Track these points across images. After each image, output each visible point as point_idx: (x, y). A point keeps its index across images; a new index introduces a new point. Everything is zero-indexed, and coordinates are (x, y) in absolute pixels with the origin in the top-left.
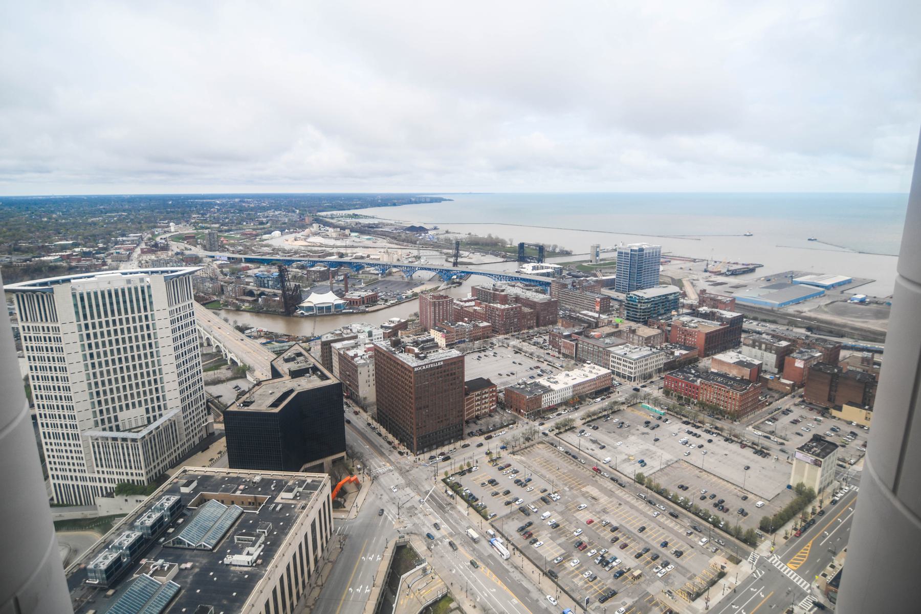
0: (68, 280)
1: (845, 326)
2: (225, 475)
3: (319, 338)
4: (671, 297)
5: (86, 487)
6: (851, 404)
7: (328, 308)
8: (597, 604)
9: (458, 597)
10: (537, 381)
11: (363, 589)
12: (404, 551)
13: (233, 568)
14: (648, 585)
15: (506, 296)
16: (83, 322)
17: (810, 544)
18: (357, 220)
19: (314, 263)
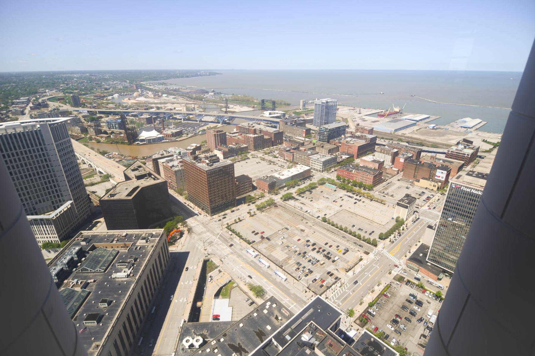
1: (425, 140)
2: (105, 233)
3: (150, 157)
4: (342, 128)
6: (424, 178)
8: (304, 278)
9: (237, 281)
10: (273, 175)
11: (189, 282)
12: (208, 263)
13: (117, 279)
14: (327, 267)
15: (255, 130)
17: (400, 243)
18: (166, 87)
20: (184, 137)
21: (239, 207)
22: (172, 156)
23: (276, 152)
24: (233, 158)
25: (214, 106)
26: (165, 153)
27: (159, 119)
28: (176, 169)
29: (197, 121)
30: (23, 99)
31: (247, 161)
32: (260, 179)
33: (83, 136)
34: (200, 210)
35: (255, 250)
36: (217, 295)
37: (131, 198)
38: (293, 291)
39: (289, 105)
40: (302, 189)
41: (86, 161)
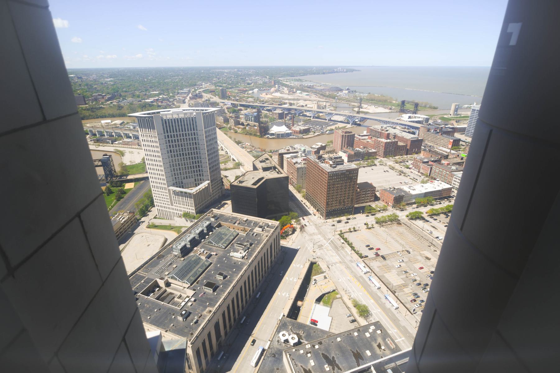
0: (159, 112)
3: (277, 151)
5: (170, 212)
7: (282, 135)
9: (341, 293)
10: (402, 187)
11: (293, 279)
15: (389, 134)
16: (166, 134)
19: (275, 109)
20: (311, 135)
21: (356, 216)
22: (297, 152)
23: (410, 162)
24: (358, 162)
25: (346, 105)
26: (291, 148)
27: (289, 115)
28: (299, 166)
29: (326, 120)
30: (186, 90)
31: (373, 167)
32: (385, 190)
33: (225, 125)
34: (315, 211)
35: (366, 266)
36: (319, 300)
37: (255, 187)
38: (403, 323)
39: (435, 108)
40: (436, 210)
41: (224, 148)
